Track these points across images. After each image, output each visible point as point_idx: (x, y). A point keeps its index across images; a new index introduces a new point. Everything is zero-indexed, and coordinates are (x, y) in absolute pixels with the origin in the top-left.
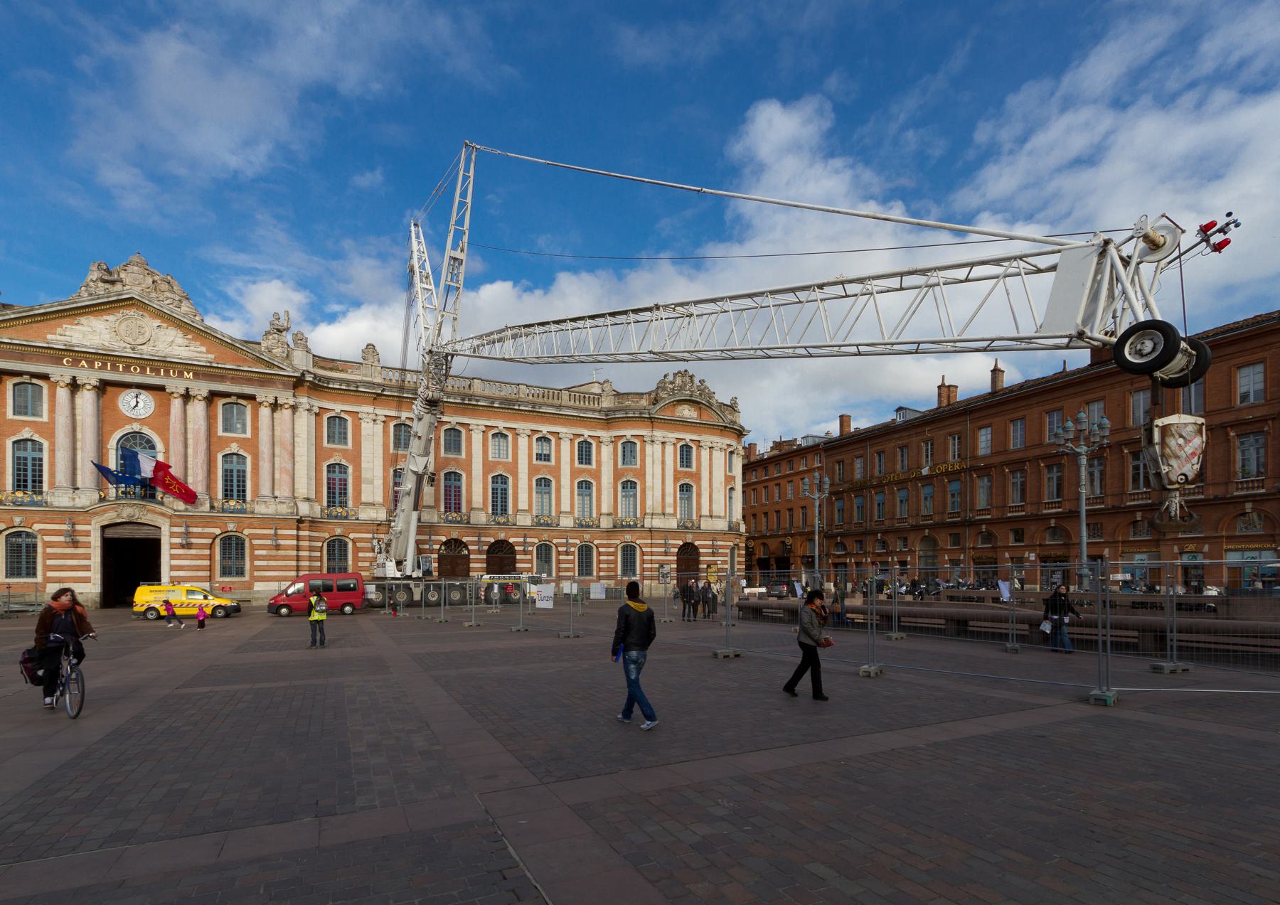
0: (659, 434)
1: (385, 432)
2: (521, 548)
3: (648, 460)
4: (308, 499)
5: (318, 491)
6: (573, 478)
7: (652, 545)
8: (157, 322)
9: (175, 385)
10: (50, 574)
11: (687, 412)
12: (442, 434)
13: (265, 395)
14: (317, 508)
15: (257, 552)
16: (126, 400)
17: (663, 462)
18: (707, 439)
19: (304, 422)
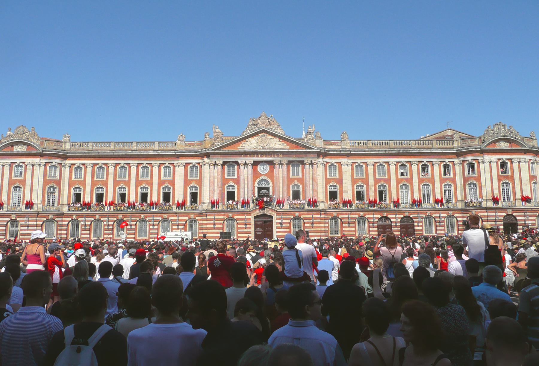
0: (487, 157)
1: (352, 169)
2: (416, 220)
3: (482, 172)
4: (323, 202)
5: (326, 198)
6: (441, 183)
7: (487, 216)
8: (271, 137)
9: (276, 160)
10: (239, 235)
11: (504, 145)
12: (377, 168)
13: (307, 160)
14: (327, 205)
15: (306, 225)
16: (260, 168)
17: (491, 172)
18: (515, 157)
19: (320, 170)
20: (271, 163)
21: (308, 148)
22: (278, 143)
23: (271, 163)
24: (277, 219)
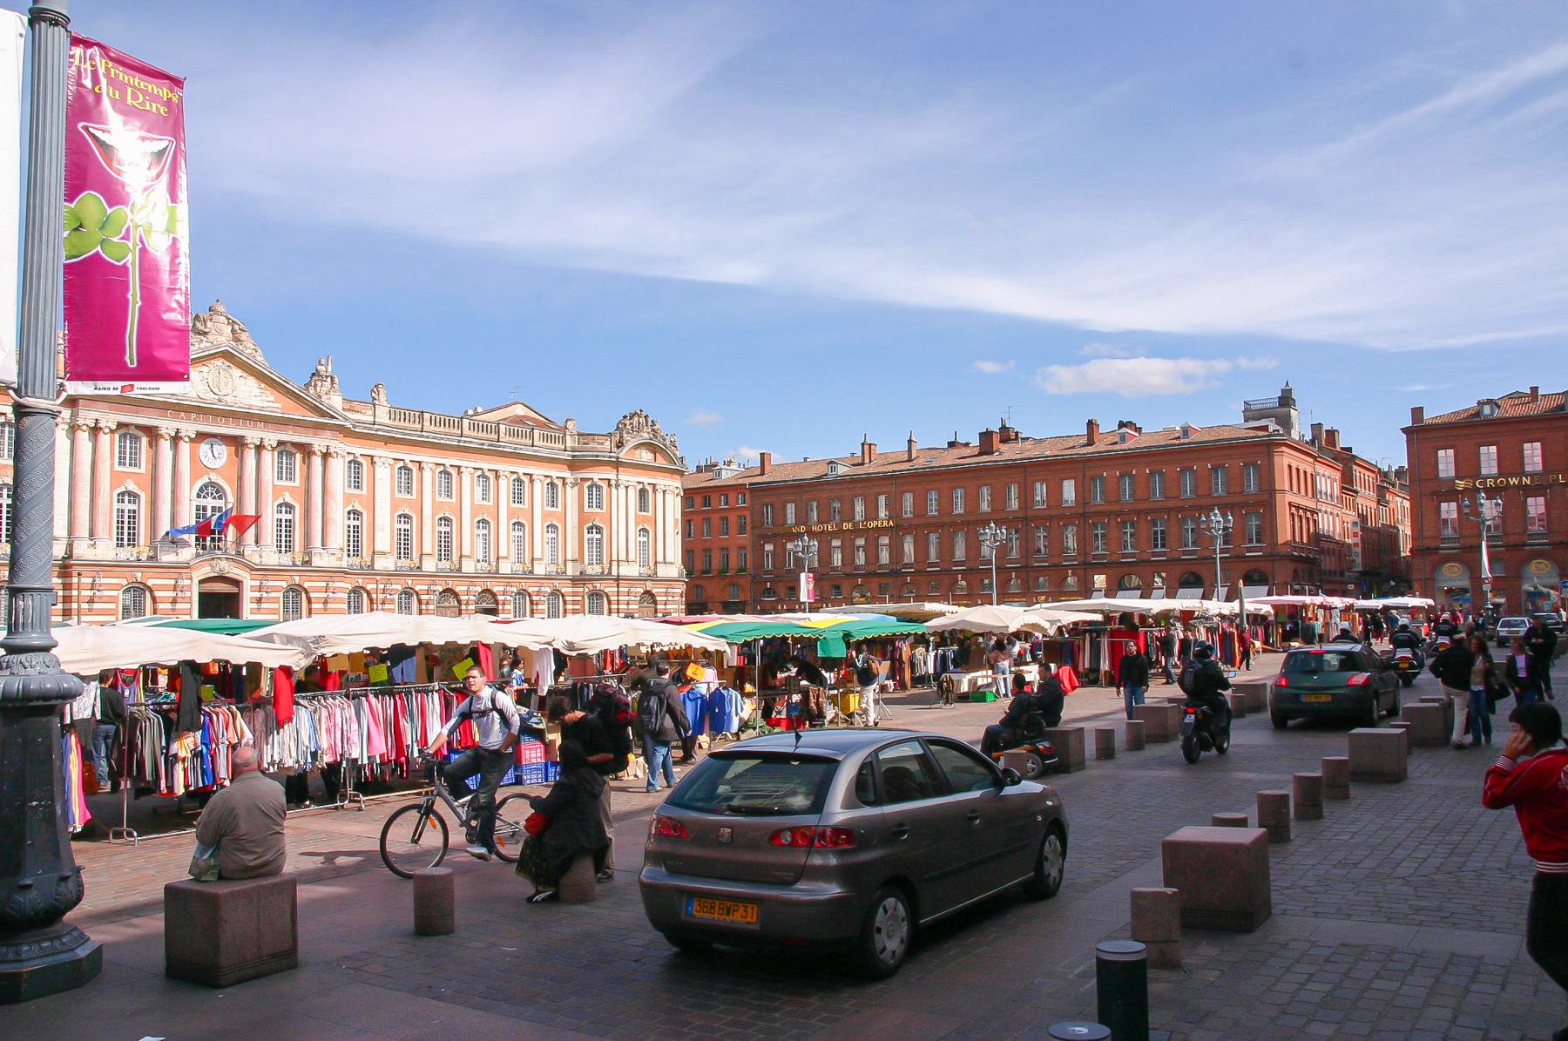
9: (252, 435)
11: (646, 456)
13: (319, 443)
16: (204, 448)
20: (237, 443)
21: (323, 414)
22: (257, 391)
23: (237, 443)
24: (253, 589)
